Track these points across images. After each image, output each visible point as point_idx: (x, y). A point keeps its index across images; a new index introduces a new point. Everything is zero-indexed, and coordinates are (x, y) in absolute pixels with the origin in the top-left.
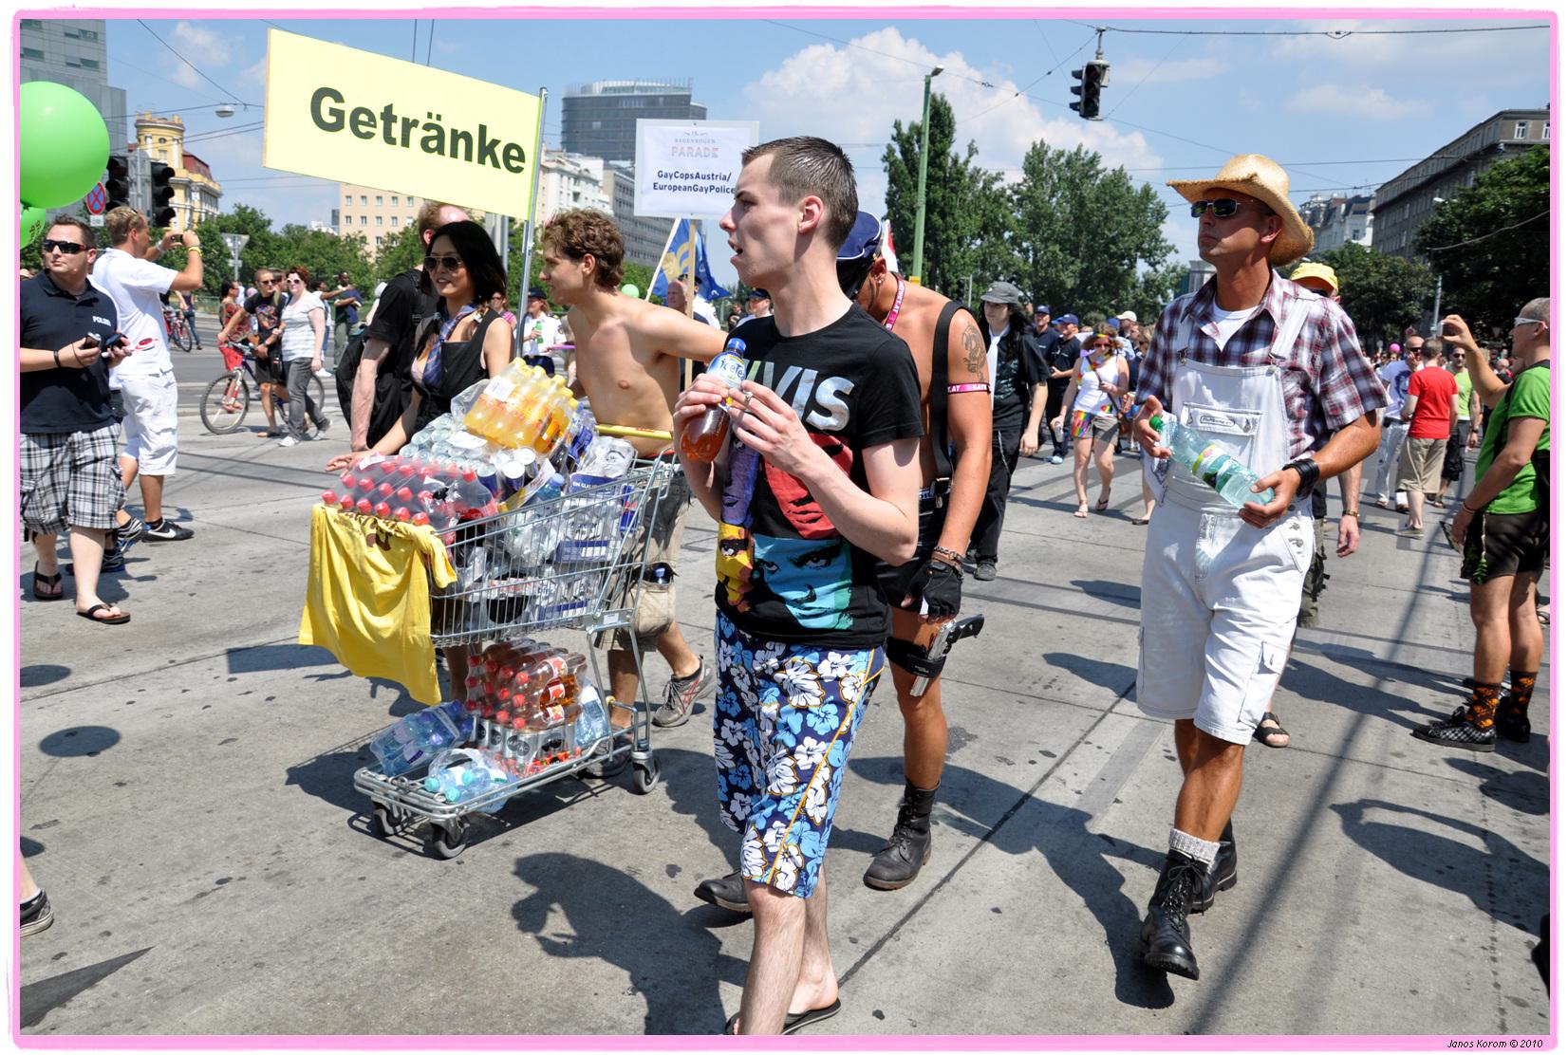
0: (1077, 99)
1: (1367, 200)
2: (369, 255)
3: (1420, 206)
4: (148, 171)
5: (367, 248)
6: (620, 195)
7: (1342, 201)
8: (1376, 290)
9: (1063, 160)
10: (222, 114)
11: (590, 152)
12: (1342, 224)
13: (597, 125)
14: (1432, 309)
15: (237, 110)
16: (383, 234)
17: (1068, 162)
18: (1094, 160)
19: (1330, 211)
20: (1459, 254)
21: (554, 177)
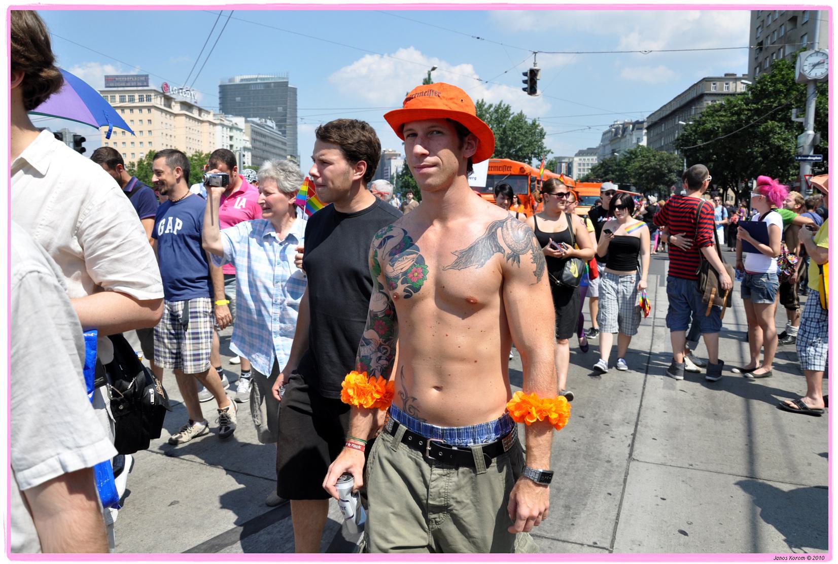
0: (526, 86)
1: (642, 123)
6: (255, 136)
7: (630, 123)
8: (655, 169)
12: (631, 135)
13: (238, 99)
17: (496, 111)
18: (507, 109)
19: (625, 129)
21: (219, 128)
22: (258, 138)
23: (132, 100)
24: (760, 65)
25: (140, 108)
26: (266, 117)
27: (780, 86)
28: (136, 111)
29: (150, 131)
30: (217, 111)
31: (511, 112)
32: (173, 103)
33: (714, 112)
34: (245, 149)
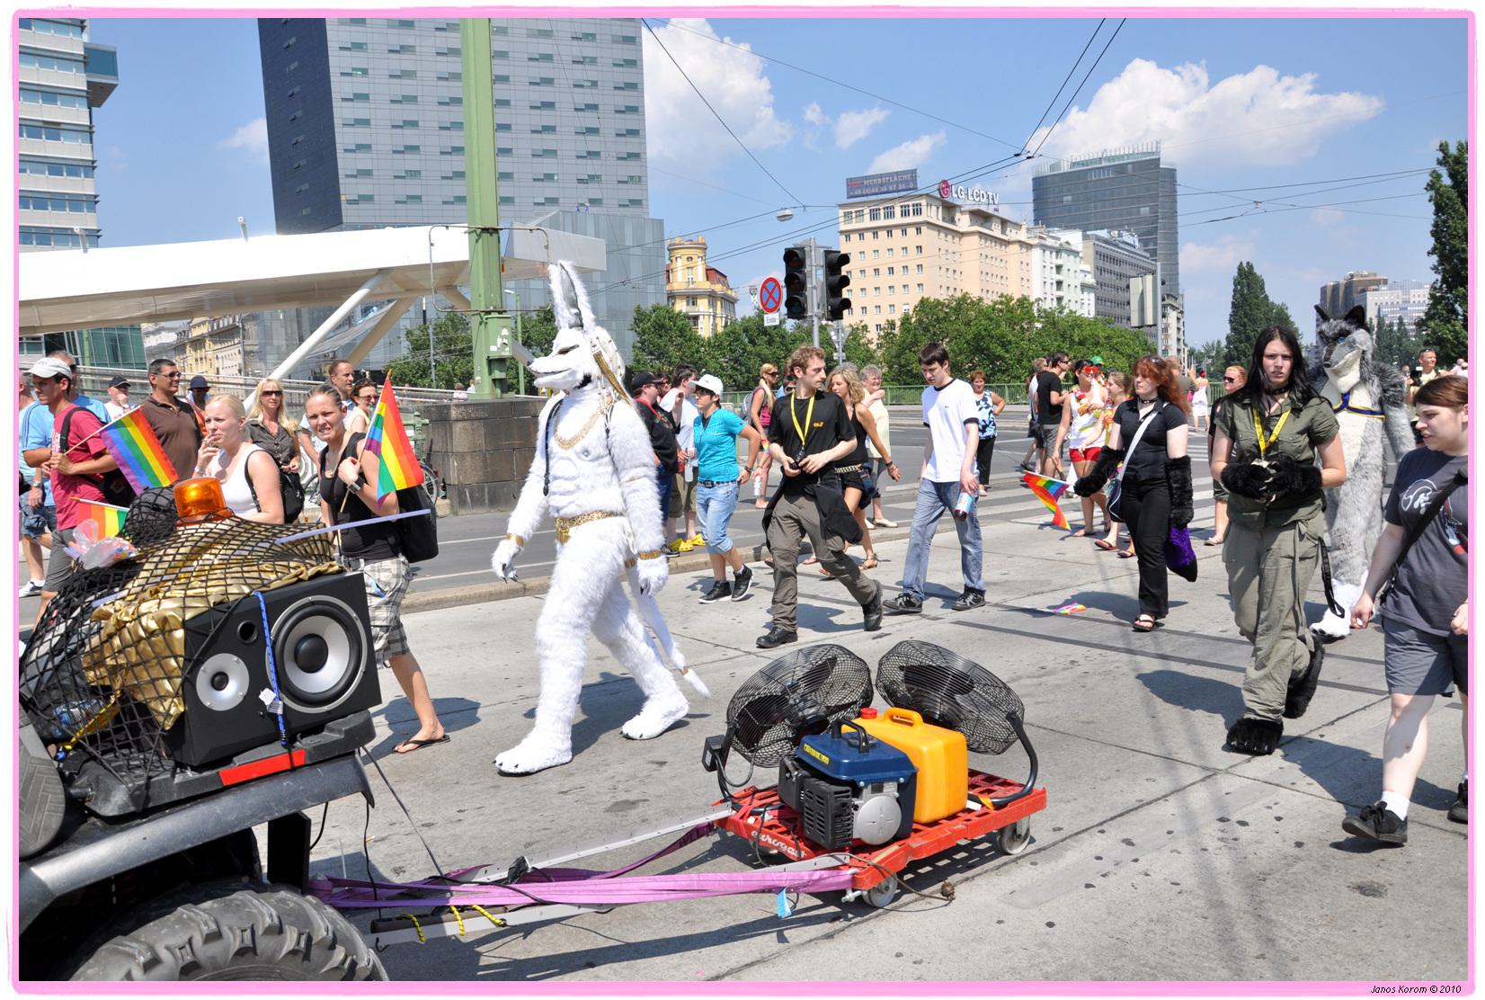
2: (870, 342)
4: (822, 262)
5: (869, 336)
6: (1101, 264)
10: (783, 218)
11: (1069, 225)
15: (797, 213)
16: (883, 323)
21: (1037, 252)
22: (1108, 266)
23: (890, 214)
25: (904, 228)
26: (1120, 227)
28: (897, 233)
29: (920, 266)
30: (1032, 225)
32: (958, 216)
34: (1084, 287)
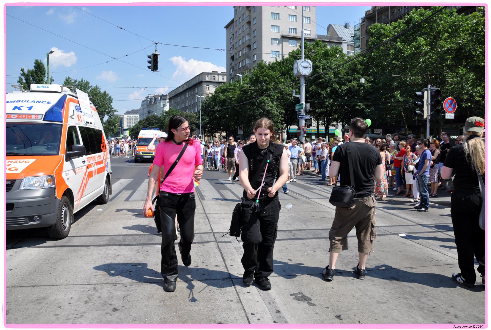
0: (150, 65)
1: (166, 95)
3: (183, 97)
7: (159, 96)
9: (77, 83)
14: (199, 128)
19: (156, 98)
20: (214, 112)
24: (233, 68)
27: (266, 78)
31: (90, 85)
33: (223, 91)
